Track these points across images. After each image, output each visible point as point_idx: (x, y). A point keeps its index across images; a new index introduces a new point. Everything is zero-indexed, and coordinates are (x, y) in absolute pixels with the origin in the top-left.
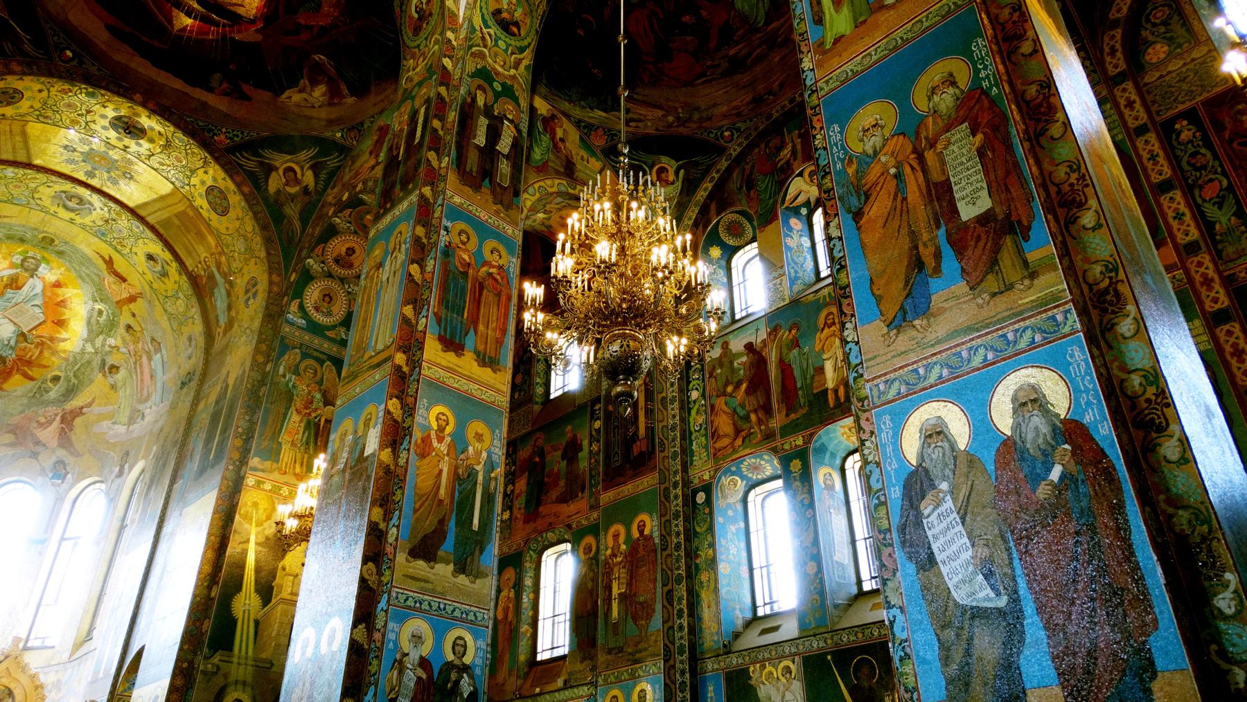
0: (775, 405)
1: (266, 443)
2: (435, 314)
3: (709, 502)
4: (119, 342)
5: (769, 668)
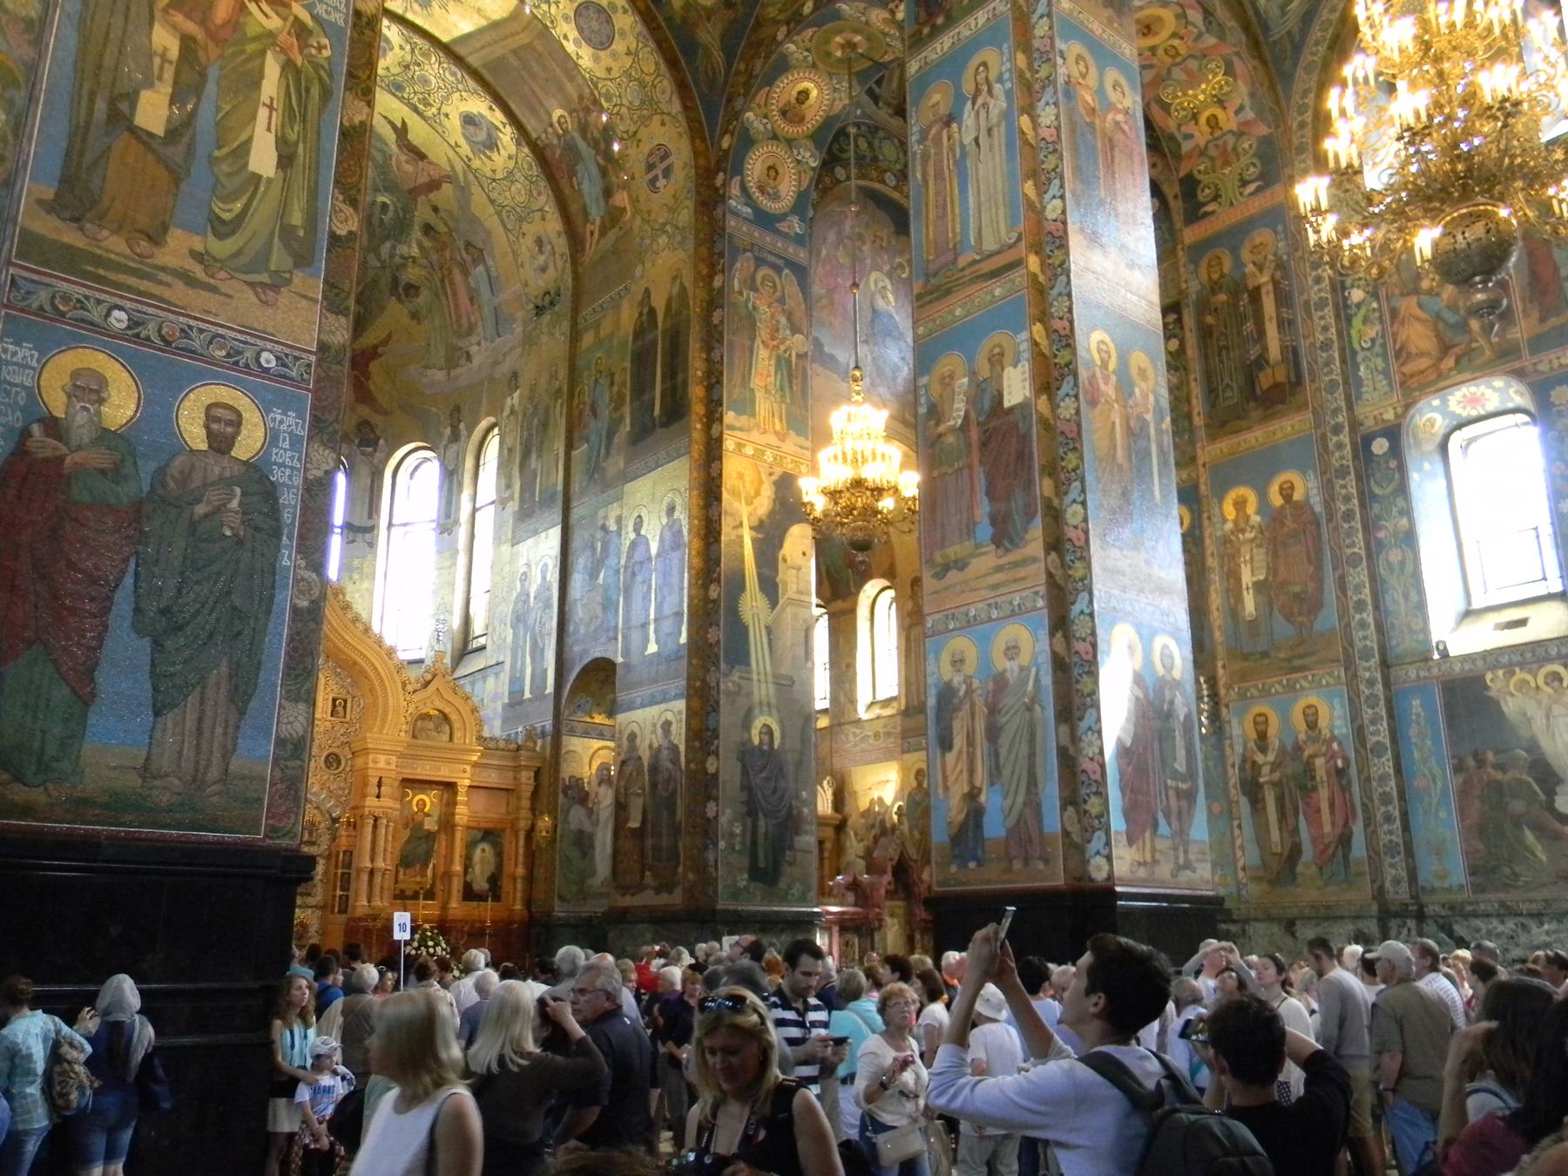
1: (737, 391)
3: (1396, 451)
4: (415, 251)
5: (1520, 675)
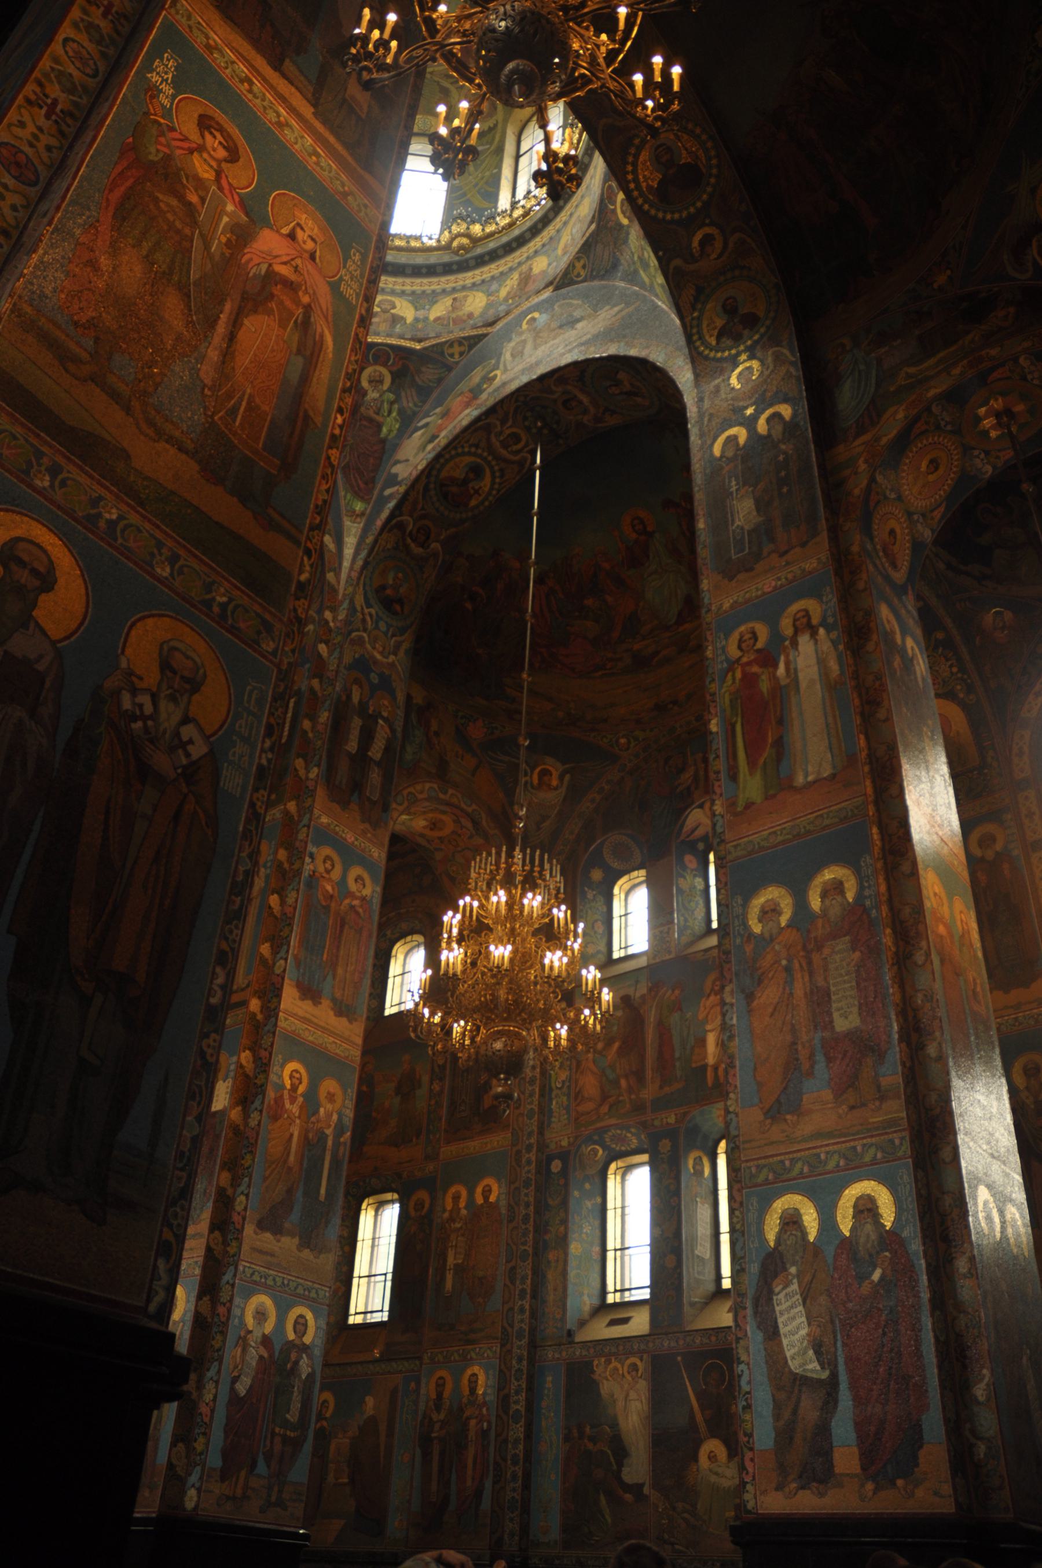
0: (649, 1074)
2: (295, 957)
3: (564, 1172)
5: (614, 1364)
